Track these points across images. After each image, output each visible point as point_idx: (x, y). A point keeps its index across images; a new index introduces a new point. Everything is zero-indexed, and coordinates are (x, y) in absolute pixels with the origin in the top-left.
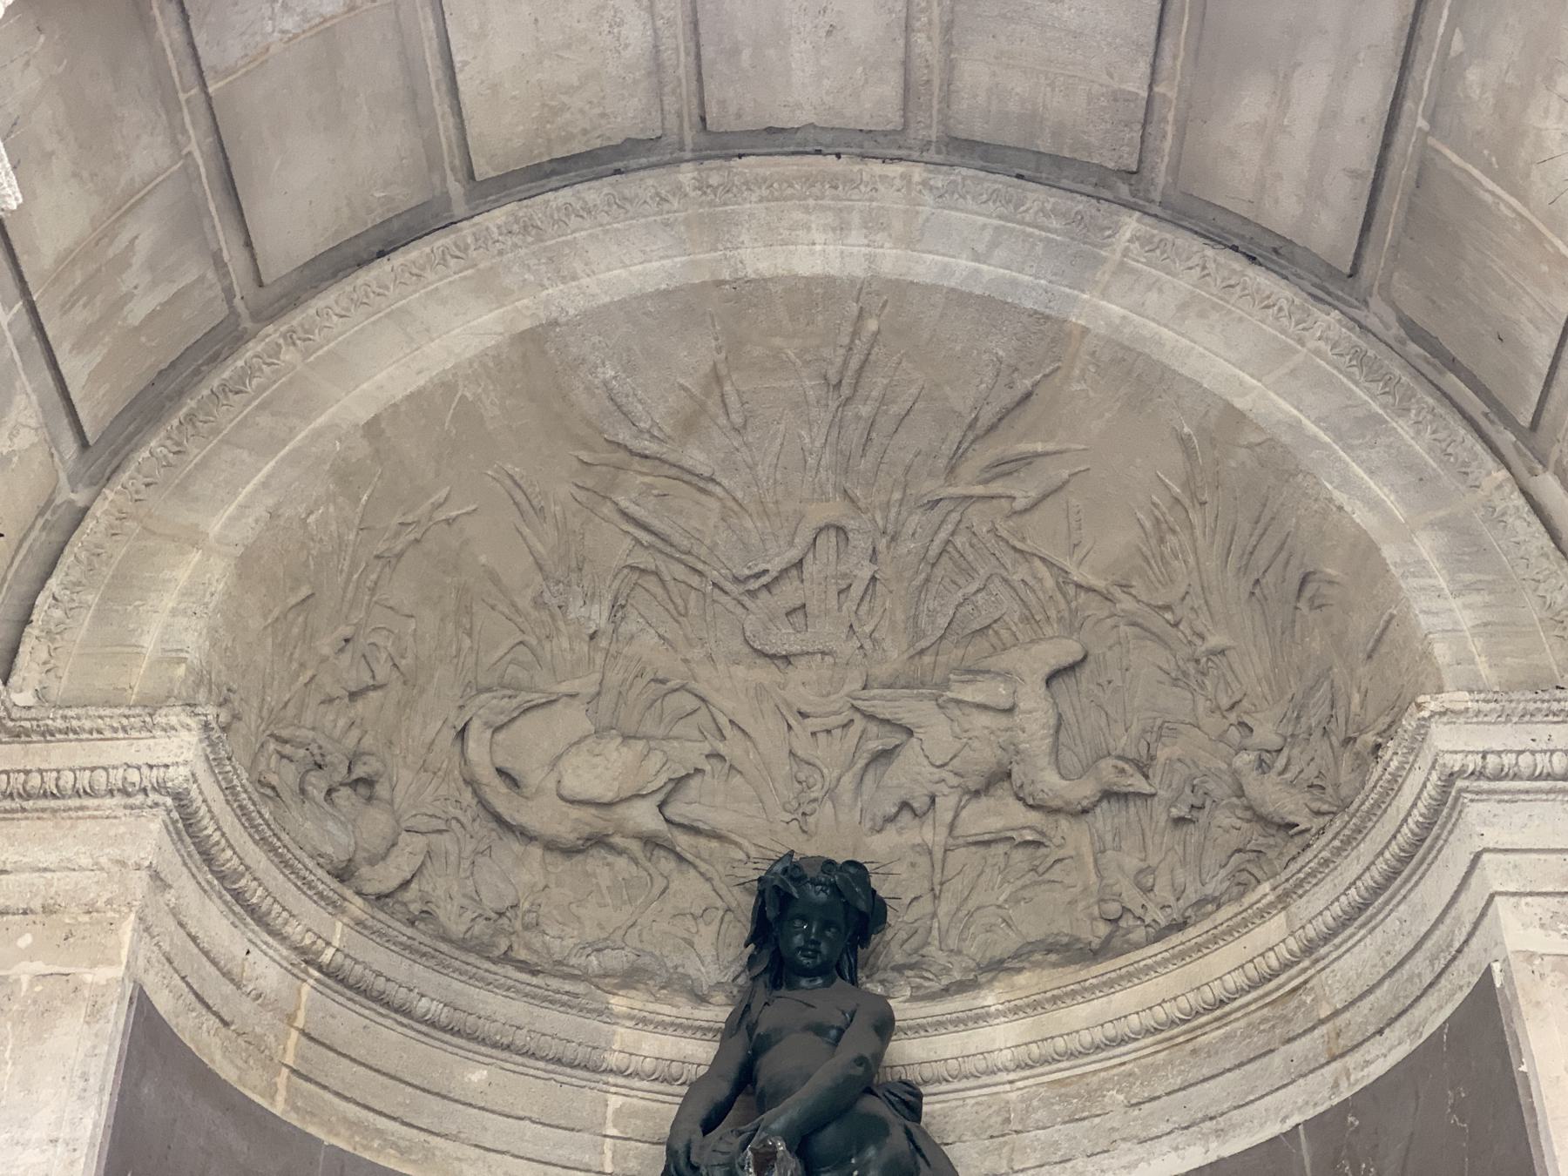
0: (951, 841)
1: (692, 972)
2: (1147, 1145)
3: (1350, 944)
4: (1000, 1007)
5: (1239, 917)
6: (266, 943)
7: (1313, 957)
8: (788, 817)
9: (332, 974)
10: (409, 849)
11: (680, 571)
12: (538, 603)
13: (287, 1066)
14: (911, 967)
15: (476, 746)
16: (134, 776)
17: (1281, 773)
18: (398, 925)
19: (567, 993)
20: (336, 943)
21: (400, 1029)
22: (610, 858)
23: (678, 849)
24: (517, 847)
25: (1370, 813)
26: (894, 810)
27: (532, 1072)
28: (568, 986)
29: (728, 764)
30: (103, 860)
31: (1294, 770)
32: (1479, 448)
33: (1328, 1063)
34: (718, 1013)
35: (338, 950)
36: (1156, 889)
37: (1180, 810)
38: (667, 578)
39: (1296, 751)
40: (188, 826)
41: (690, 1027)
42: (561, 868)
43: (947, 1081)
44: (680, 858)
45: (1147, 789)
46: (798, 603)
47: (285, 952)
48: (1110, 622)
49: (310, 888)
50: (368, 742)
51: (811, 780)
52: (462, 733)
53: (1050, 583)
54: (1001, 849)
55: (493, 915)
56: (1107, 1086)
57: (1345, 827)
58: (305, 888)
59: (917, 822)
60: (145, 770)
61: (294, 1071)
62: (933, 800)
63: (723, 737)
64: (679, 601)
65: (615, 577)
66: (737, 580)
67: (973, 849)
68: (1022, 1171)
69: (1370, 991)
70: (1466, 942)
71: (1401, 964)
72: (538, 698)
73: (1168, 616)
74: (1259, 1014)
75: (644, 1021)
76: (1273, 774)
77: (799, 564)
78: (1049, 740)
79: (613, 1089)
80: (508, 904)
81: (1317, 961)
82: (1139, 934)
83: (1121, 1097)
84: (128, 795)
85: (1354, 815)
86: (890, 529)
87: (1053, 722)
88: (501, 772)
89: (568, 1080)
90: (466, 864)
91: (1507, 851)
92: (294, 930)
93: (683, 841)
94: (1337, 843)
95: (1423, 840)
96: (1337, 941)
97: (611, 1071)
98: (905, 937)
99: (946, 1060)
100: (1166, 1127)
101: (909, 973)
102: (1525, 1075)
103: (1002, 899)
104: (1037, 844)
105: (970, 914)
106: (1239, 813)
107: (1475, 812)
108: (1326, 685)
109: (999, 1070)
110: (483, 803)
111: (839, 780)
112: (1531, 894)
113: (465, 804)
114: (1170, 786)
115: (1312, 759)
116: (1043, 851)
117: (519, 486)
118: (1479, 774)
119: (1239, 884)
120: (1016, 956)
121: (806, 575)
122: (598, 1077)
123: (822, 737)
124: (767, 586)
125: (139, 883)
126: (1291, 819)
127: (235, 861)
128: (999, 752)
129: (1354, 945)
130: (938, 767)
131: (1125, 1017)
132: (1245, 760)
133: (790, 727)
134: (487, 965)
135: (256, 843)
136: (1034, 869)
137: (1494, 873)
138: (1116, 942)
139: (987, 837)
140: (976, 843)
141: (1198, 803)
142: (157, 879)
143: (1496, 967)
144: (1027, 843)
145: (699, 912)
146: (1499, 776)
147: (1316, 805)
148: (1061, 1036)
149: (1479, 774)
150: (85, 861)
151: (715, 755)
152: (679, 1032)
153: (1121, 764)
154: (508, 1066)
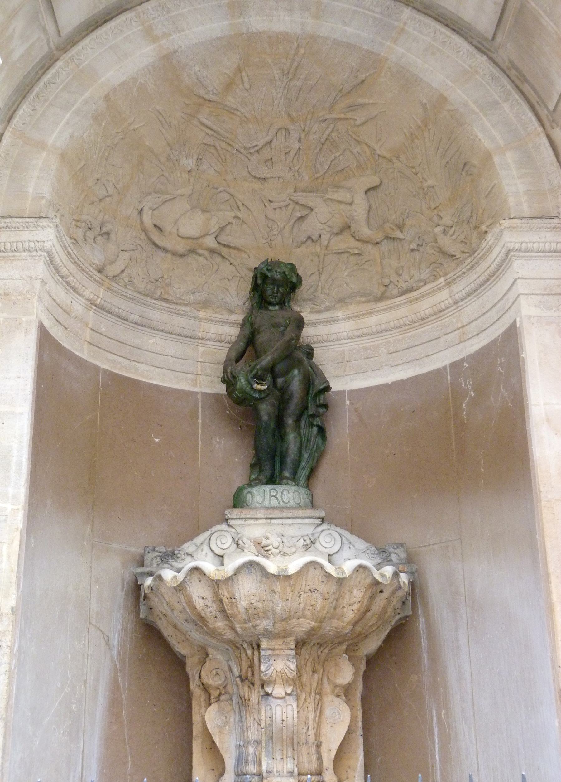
0: (326, 252)
1: (229, 302)
2: (394, 368)
3: (470, 302)
4: (343, 317)
5: (432, 289)
6: (77, 298)
7: (458, 305)
8: (264, 241)
10: (123, 258)
11: (223, 145)
12: (168, 159)
13: (87, 341)
14: (310, 300)
15: (147, 218)
16: (32, 245)
17: (451, 236)
18: (121, 288)
19: (183, 311)
20: (101, 297)
21: (124, 325)
22: (197, 257)
23: (223, 254)
24: (162, 254)
25: (481, 258)
26: (305, 240)
27: (171, 339)
28: (183, 308)
29: (241, 220)
30: (24, 276)
31: (456, 234)
32: (533, 118)
33: (459, 343)
34: (239, 318)
35: (102, 299)
36: (403, 274)
37: (414, 246)
38: (218, 148)
39: (458, 228)
40: (51, 261)
41: (228, 323)
42: (178, 262)
43: (323, 343)
44: (223, 257)
45: (401, 236)
46: (270, 157)
47: (84, 301)
48: (391, 171)
49: (91, 277)
50: (106, 217)
51: (273, 227)
52: (141, 212)
54: (346, 255)
56: (381, 346)
57: (472, 262)
58: (90, 278)
59: (314, 244)
60: (36, 243)
61: (89, 343)
62: (320, 236)
63: (240, 210)
64: (223, 157)
65: (198, 148)
66: (245, 148)
67: (335, 255)
68: (348, 375)
69: (476, 319)
70: (509, 308)
71: (487, 312)
72: (168, 197)
73: (414, 170)
74: (436, 324)
75: (211, 320)
76: (448, 236)
78: (365, 216)
79: (201, 345)
80: (160, 276)
81: (458, 307)
82: (395, 292)
83: (386, 351)
84: (30, 252)
85: (475, 258)
86: (307, 129)
87: (367, 208)
88: (155, 226)
89: (184, 342)
90: (143, 262)
91: (526, 278)
92: (87, 293)
93: (224, 250)
94: (468, 267)
95: (498, 270)
96: (466, 300)
97: (200, 338)
98: (308, 288)
99: (322, 335)
100: (401, 362)
101: (309, 302)
102: (523, 357)
103: (346, 274)
104: (359, 255)
105: (333, 280)
106: (435, 249)
107: (517, 264)
108: (470, 204)
109: (342, 339)
110: (149, 239)
112: (533, 294)
113: (142, 238)
114: (410, 235)
115: (463, 232)
116: (362, 257)
118: (520, 250)
119: (433, 275)
120: (350, 297)
121: (273, 147)
122: (194, 341)
123: (278, 210)
124: (258, 151)
125: (37, 285)
126: (453, 253)
127: (67, 271)
128: (346, 219)
129: (472, 303)
130: (322, 224)
131: (389, 322)
132: (438, 230)
133: (265, 206)
134: (153, 301)
135: (73, 264)
136: (357, 264)
137: (520, 287)
138: (388, 294)
139: (340, 251)
140: (336, 253)
141: (420, 243)
142: (43, 282)
143: (518, 319)
144: (355, 254)
145: (230, 278)
146: (527, 251)
147: (463, 249)
148: (365, 328)
149: (520, 250)
150: (18, 276)
151: (236, 217)
152: (224, 324)
153: (392, 226)
154: (163, 337)
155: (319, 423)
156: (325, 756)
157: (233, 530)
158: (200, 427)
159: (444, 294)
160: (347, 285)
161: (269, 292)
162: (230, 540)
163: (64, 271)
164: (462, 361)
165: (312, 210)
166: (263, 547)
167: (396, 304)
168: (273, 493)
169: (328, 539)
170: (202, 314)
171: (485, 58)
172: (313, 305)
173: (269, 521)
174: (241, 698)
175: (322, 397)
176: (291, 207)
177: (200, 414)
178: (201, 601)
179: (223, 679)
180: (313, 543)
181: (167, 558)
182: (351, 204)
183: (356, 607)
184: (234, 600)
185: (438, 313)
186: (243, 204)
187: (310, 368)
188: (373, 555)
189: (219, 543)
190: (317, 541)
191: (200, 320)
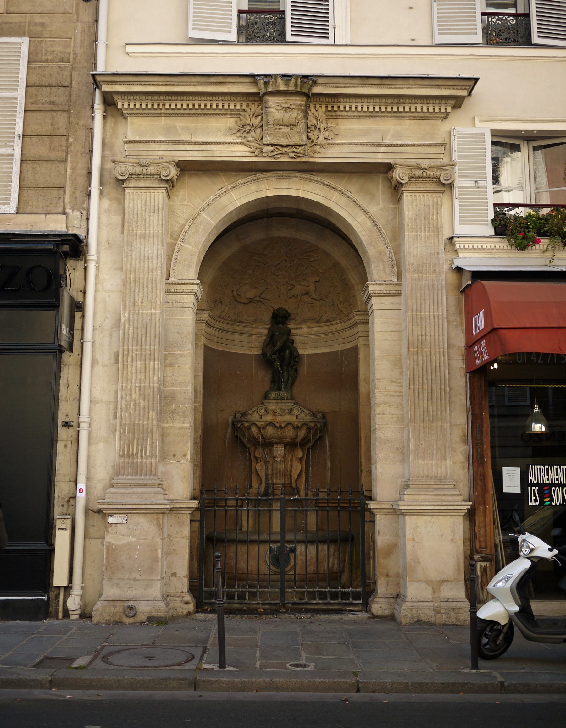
24: (240, 304)
52: (233, 291)
93: (262, 300)
107: (359, 326)
156: (293, 479)
159: (339, 325)
164: (343, 350)
165: (295, 286)
170: (254, 326)
175: (296, 359)
183: (303, 435)
185: (338, 331)
191: (254, 328)
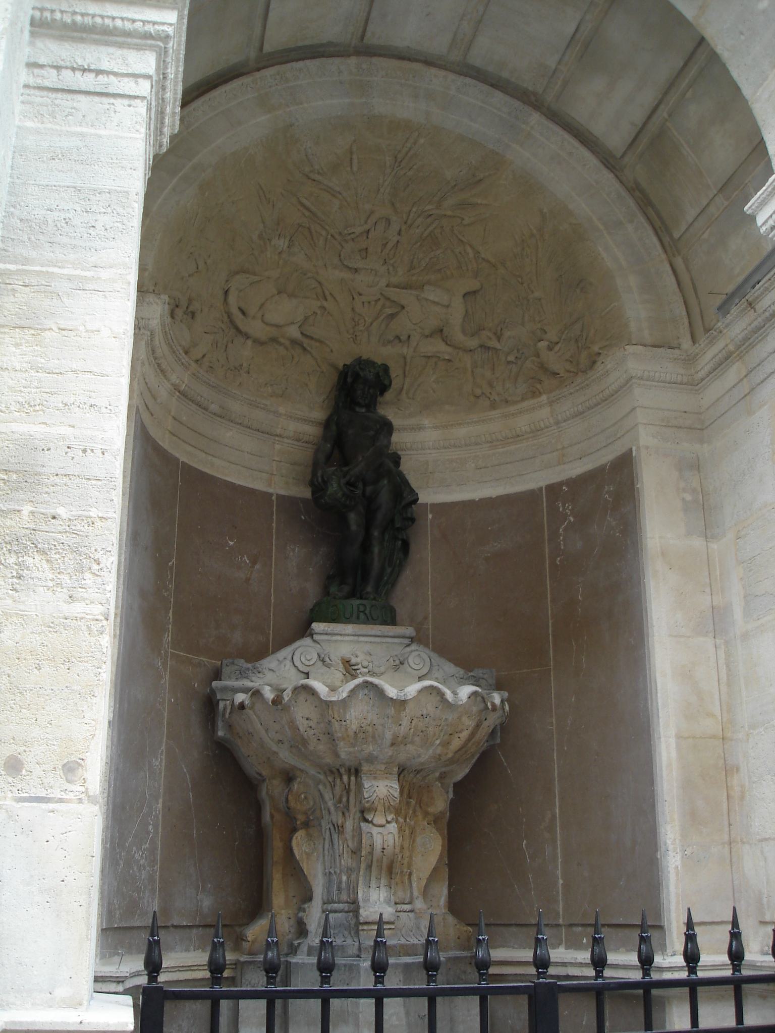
9: (183, 394)
17: (556, 353)
20: (186, 382)
44: (304, 349)
45: (498, 346)
46: (365, 247)
52: (226, 293)
53: (471, 255)
55: (233, 369)
62: (409, 337)
63: (326, 300)
66: (340, 234)
72: (256, 278)
75: (291, 417)
77: (368, 232)
93: (306, 342)
94: (577, 388)
95: (613, 395)
102: (638, 488)
103: (432, 380)
111: (372, 324)
117: (262, 189)
118: (641, 378)
121: (370, 236)
124: (353, 240)
126: (557, 371)
130: (414, 324)
133: (353, 298)
143: (634, 449)
144: (445, 359)
149: (641, 378)
151: (323, 308)
155: (405, 537)
157: (319, 646)
158: (274, 531)
160: (434, 392)
161: (359, 392)
162: (315, 657)
163: (159, 352)
164: (561, 484)
165: (403, 307)
166: (351, 666)
167: (490, 417)
168: (362, 609)
169: (417, 661)
171: (611, 176)
172: (397, 410)
173: (356, 638)
174: (334, 825)
176: (380, 303)
177: (274, 517)
178: (306, 722)
179: (312, 803)
180: (402, 663)
181: (247, 672)
182: (448, 306)
184: (344, 723)
186: (331, 294)
187: (398, 478)
188: (462, 680)
189: (303, 659)
190: (406, 662)
